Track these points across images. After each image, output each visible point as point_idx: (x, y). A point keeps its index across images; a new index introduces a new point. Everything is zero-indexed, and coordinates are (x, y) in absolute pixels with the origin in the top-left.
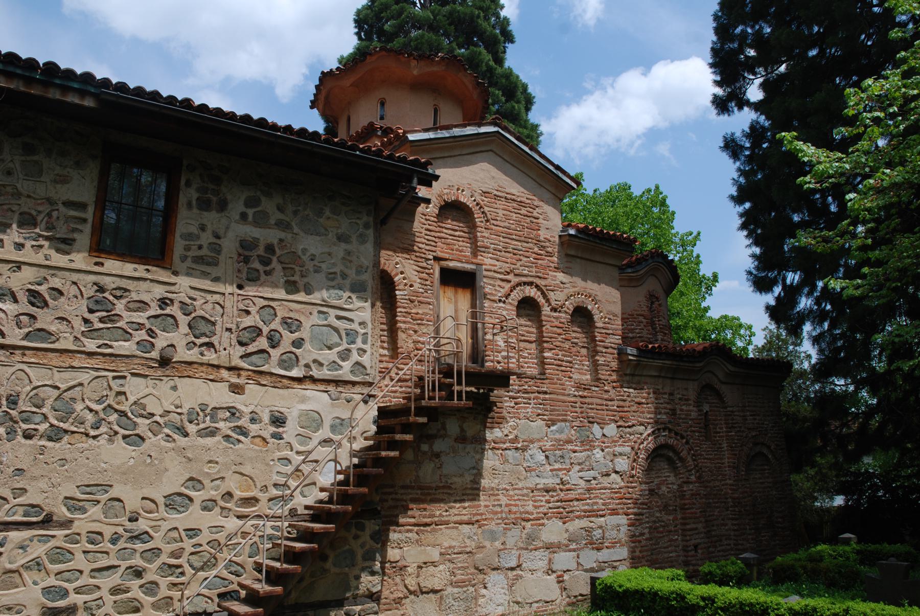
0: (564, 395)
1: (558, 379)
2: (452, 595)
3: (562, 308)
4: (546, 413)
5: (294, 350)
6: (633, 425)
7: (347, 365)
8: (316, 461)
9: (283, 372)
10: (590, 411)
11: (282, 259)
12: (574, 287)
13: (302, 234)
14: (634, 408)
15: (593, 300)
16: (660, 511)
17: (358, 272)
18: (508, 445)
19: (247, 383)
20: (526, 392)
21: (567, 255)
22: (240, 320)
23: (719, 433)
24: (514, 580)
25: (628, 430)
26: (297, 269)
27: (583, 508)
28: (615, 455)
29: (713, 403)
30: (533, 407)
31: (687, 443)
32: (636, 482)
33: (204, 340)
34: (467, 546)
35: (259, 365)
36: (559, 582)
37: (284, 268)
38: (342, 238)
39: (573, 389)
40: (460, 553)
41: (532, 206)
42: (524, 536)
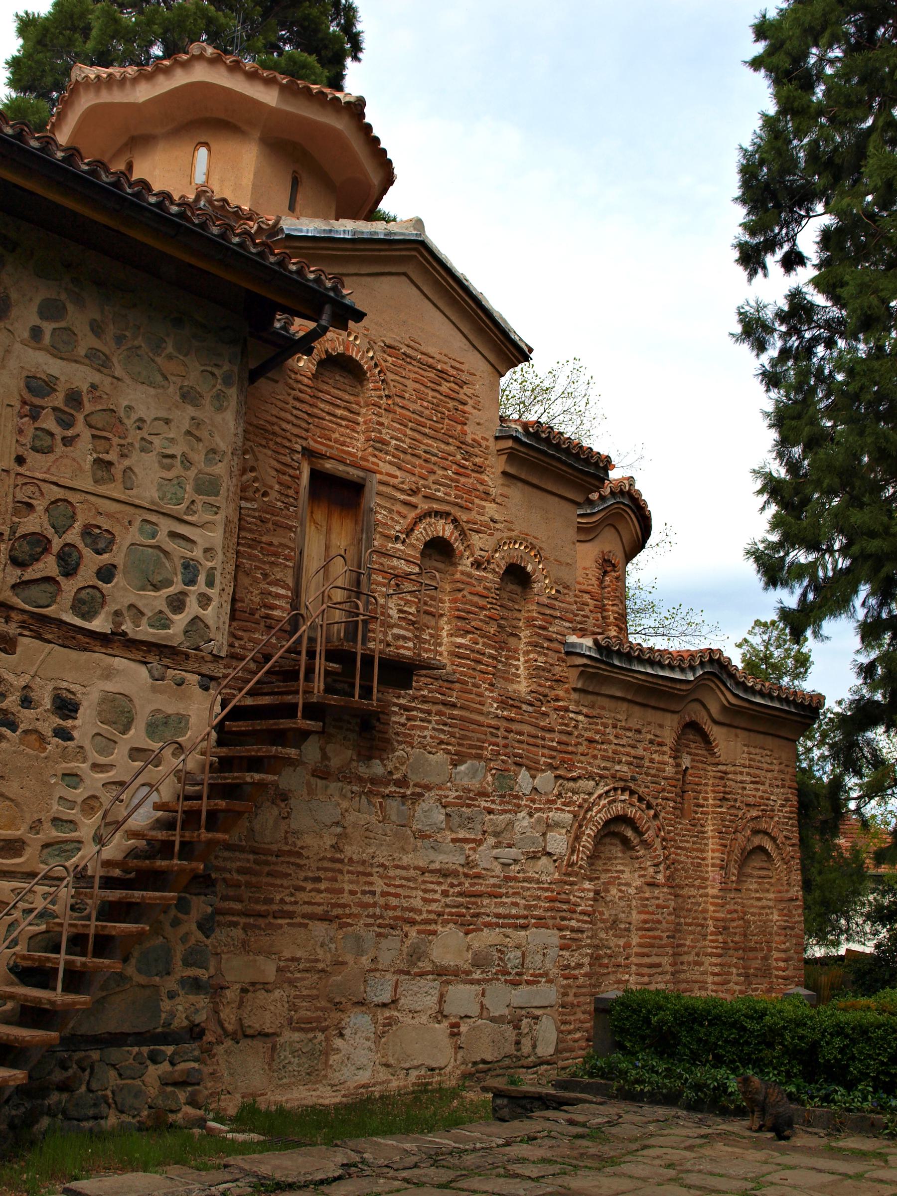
0: (481, 713)
1: (474, 685)
2: (291, 1044)
3: (489, 562)
6: (579, 777)
7: (180, 621)
8: (121, 784)
9: (78, 622)
10: (517, 745)
11: (93, 420)
12: (510, 530)
13: (128, 380)
14: (581, 749)
15: (535, 556)
16: (606, 930)
17: (208, 461)
18: (393, 789)
19: (21, 635)
20: (425, 700)
21: (505, 473)
22: (17, 520)
24: (384, 1025)
25: (571, 784)
26: (116, 441)
27: (497, 911)
28: (548, 825)
29: (697, 755)
30: (434, 729)
31: (656, 816)
32: (576, 874)
34: (317, 961)
35: (41, 603)
36: (453, 1035)
37: (94, 436)
38: (188, 396)
39: (495, 705)
40: (307, 971)
42: (405, 950)
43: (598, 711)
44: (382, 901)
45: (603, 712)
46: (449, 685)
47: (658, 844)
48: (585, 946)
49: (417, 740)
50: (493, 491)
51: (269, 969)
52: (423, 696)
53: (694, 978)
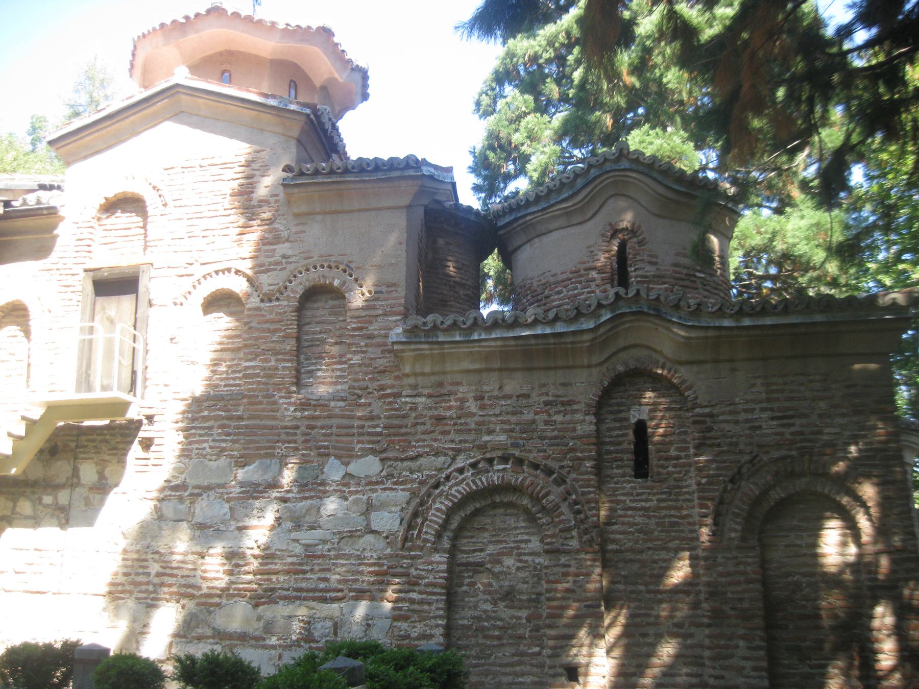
0: (274, 418)
1: (264, 397)
4: (237, 445)
12: (306, 259)
14: (428, 427)
16: (495, 603)
23: (677, 458)
25: (409, 463)
27: (299, 585)
30: (214, 441)
32: (421, 549)
43: (450, 388)
46: (235, 402)
47: (564, 508)
50: (285, 234)
52: (204, 417)
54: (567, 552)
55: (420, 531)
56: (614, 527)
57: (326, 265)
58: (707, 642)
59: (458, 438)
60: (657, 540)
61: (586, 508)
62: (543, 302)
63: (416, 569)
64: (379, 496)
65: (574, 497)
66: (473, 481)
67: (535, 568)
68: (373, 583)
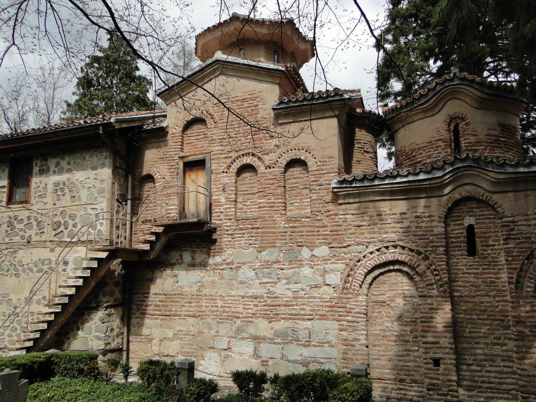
1: (269, 217)
5: (73, 228)
10: (299, 237)
14: (353, 230)
18: (225, 266)
23: (493, 245)
24: (225, 358)
25: (344, 249)
26: (75, 189)
27: (291, 312)
29: (482, 215)
30: (246, 240)
32: (352, 294)
33: (42, 231)
34: (190, 331)
39: (283, 223)
41: (253, 98)
42: (234, 328)
44: (221, 309)
45: (366, 210)
46: (255, 220)
47: (428, 273)
48: (360, 330)
49: (237, 246)
51: (170, 334)
53: (493, 353)
54: (431, 297)
55: (351, 285)
56: (458, 283)
57: (297, 148)
58: (515, 349)
59: (369, 236)
60: (483, 291)
61: (441, 273)
62: (412, 159)
63: (350, 304)
64: (329, 266)
65: (434, 267)
66: (378, 259)
67: (413, 304)
68: (328, 311)
